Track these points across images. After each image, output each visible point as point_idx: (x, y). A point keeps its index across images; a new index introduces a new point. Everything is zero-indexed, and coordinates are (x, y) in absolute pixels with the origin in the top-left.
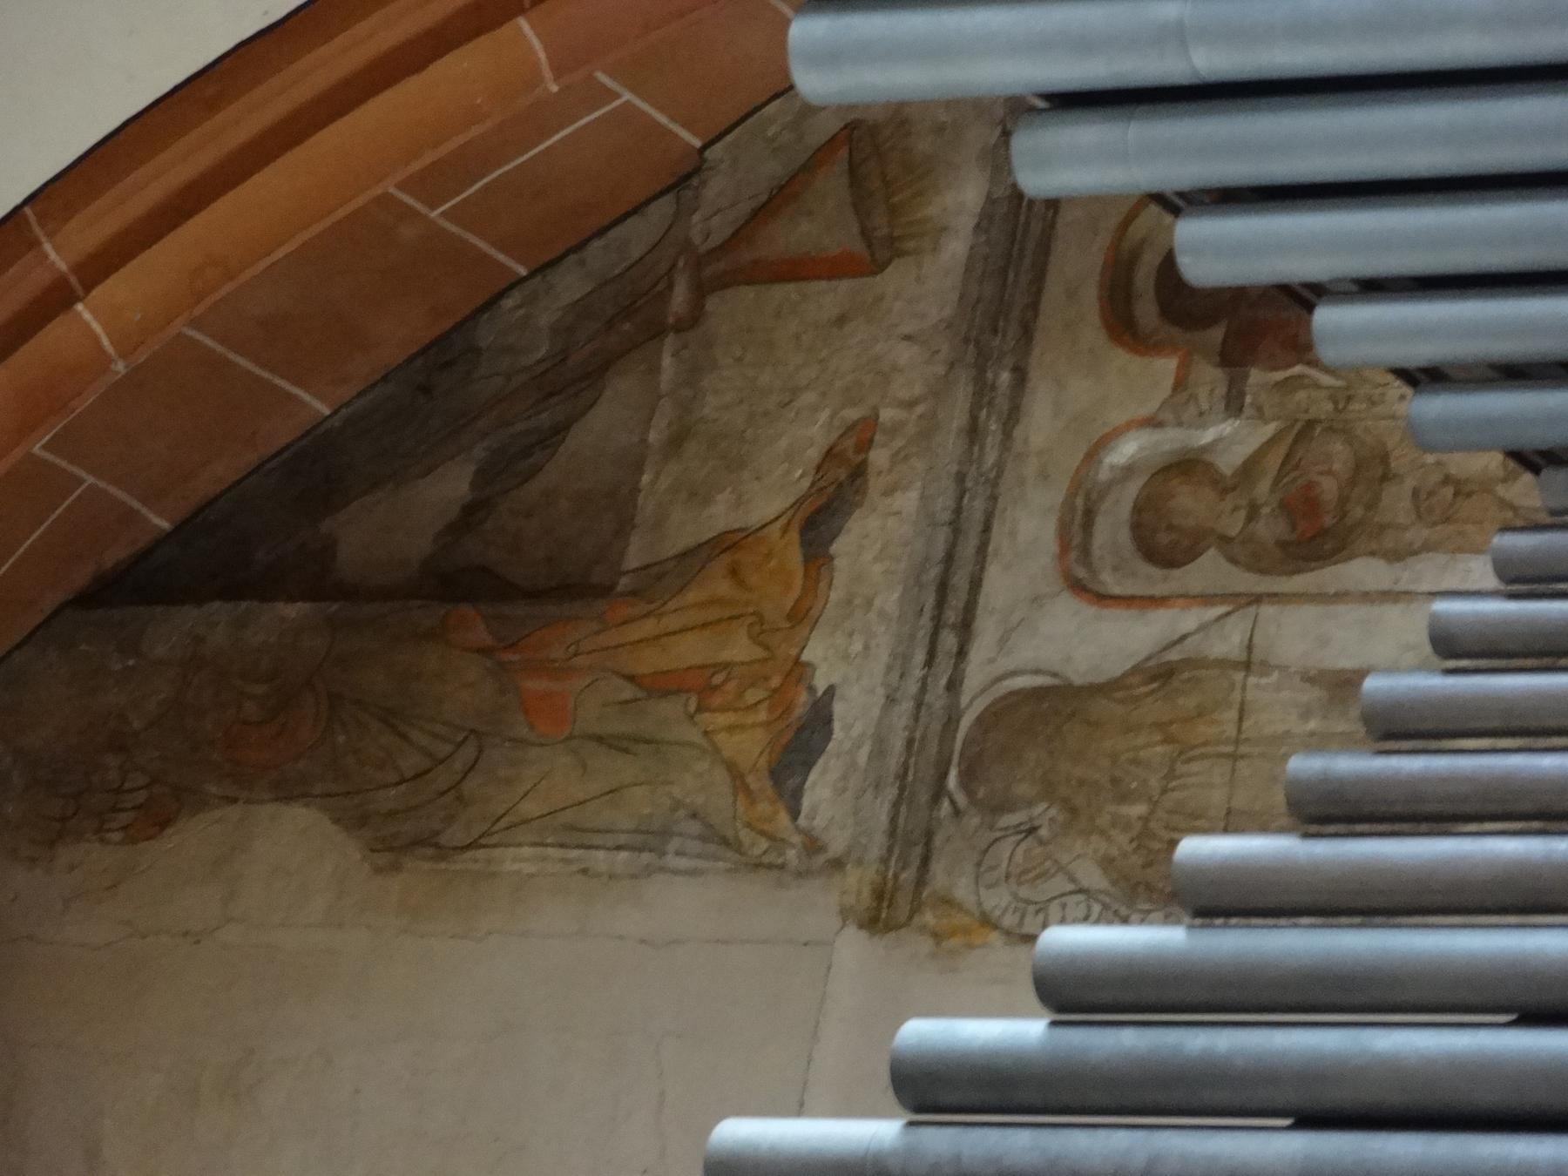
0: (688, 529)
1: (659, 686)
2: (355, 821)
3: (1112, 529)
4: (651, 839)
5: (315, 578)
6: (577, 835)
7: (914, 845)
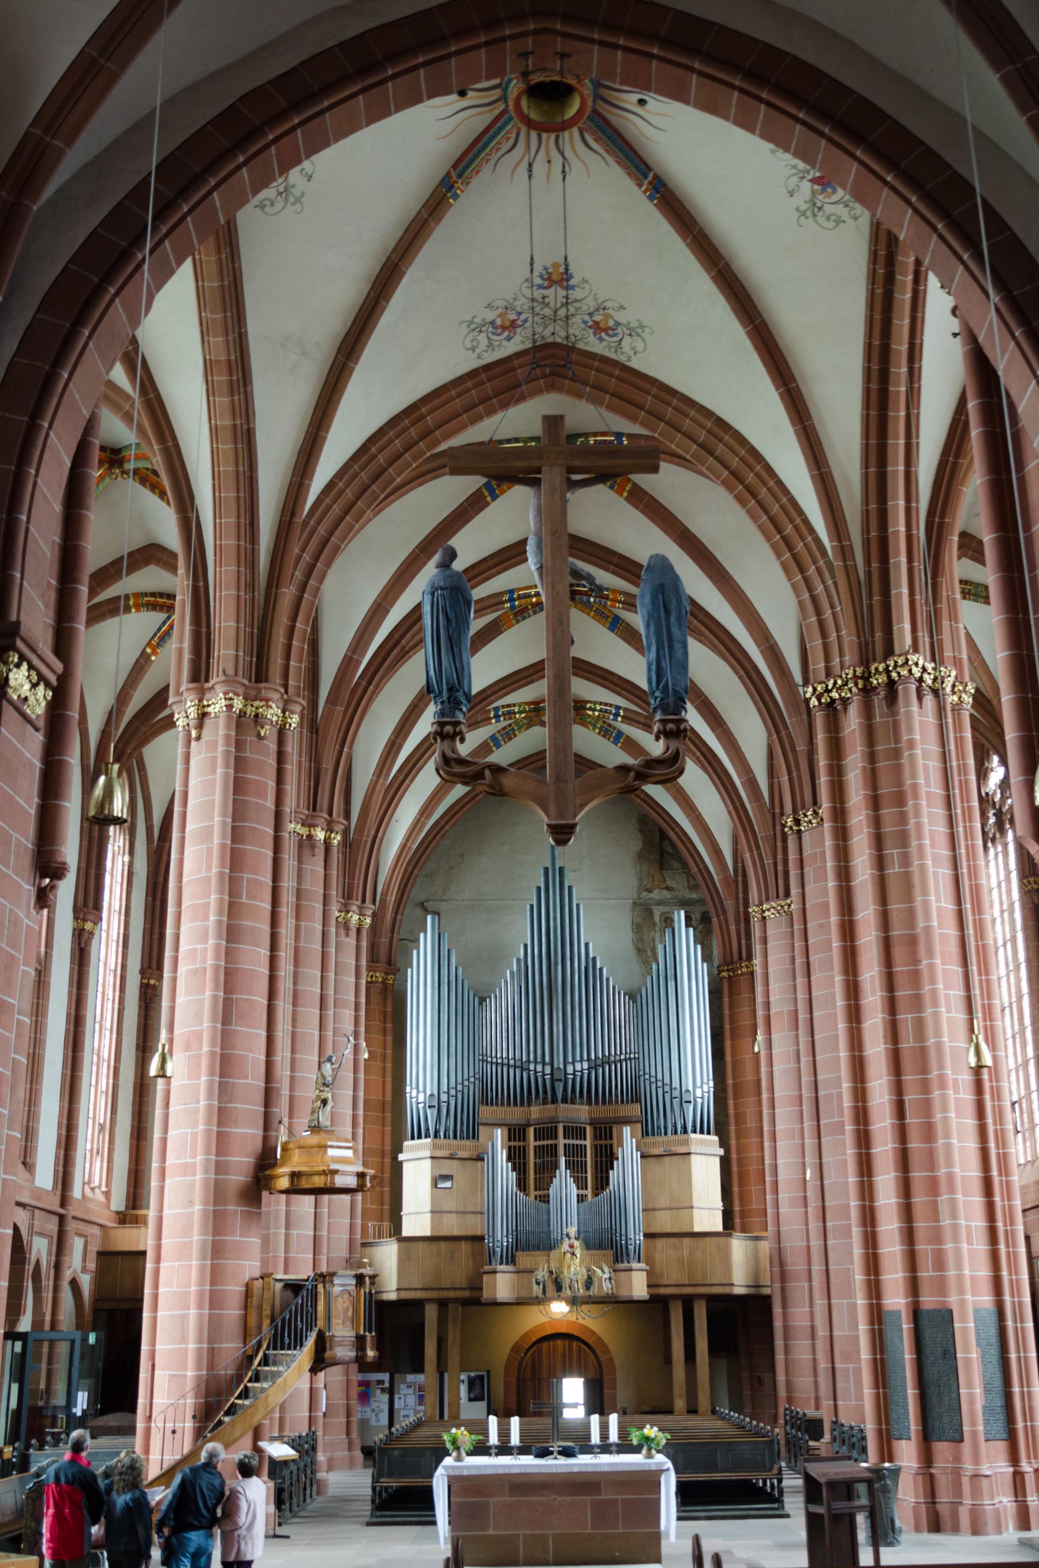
0: (666, 876)
4: (641, 879)
5: (661, 841)
6: (641, 871)
7: (640, 905)
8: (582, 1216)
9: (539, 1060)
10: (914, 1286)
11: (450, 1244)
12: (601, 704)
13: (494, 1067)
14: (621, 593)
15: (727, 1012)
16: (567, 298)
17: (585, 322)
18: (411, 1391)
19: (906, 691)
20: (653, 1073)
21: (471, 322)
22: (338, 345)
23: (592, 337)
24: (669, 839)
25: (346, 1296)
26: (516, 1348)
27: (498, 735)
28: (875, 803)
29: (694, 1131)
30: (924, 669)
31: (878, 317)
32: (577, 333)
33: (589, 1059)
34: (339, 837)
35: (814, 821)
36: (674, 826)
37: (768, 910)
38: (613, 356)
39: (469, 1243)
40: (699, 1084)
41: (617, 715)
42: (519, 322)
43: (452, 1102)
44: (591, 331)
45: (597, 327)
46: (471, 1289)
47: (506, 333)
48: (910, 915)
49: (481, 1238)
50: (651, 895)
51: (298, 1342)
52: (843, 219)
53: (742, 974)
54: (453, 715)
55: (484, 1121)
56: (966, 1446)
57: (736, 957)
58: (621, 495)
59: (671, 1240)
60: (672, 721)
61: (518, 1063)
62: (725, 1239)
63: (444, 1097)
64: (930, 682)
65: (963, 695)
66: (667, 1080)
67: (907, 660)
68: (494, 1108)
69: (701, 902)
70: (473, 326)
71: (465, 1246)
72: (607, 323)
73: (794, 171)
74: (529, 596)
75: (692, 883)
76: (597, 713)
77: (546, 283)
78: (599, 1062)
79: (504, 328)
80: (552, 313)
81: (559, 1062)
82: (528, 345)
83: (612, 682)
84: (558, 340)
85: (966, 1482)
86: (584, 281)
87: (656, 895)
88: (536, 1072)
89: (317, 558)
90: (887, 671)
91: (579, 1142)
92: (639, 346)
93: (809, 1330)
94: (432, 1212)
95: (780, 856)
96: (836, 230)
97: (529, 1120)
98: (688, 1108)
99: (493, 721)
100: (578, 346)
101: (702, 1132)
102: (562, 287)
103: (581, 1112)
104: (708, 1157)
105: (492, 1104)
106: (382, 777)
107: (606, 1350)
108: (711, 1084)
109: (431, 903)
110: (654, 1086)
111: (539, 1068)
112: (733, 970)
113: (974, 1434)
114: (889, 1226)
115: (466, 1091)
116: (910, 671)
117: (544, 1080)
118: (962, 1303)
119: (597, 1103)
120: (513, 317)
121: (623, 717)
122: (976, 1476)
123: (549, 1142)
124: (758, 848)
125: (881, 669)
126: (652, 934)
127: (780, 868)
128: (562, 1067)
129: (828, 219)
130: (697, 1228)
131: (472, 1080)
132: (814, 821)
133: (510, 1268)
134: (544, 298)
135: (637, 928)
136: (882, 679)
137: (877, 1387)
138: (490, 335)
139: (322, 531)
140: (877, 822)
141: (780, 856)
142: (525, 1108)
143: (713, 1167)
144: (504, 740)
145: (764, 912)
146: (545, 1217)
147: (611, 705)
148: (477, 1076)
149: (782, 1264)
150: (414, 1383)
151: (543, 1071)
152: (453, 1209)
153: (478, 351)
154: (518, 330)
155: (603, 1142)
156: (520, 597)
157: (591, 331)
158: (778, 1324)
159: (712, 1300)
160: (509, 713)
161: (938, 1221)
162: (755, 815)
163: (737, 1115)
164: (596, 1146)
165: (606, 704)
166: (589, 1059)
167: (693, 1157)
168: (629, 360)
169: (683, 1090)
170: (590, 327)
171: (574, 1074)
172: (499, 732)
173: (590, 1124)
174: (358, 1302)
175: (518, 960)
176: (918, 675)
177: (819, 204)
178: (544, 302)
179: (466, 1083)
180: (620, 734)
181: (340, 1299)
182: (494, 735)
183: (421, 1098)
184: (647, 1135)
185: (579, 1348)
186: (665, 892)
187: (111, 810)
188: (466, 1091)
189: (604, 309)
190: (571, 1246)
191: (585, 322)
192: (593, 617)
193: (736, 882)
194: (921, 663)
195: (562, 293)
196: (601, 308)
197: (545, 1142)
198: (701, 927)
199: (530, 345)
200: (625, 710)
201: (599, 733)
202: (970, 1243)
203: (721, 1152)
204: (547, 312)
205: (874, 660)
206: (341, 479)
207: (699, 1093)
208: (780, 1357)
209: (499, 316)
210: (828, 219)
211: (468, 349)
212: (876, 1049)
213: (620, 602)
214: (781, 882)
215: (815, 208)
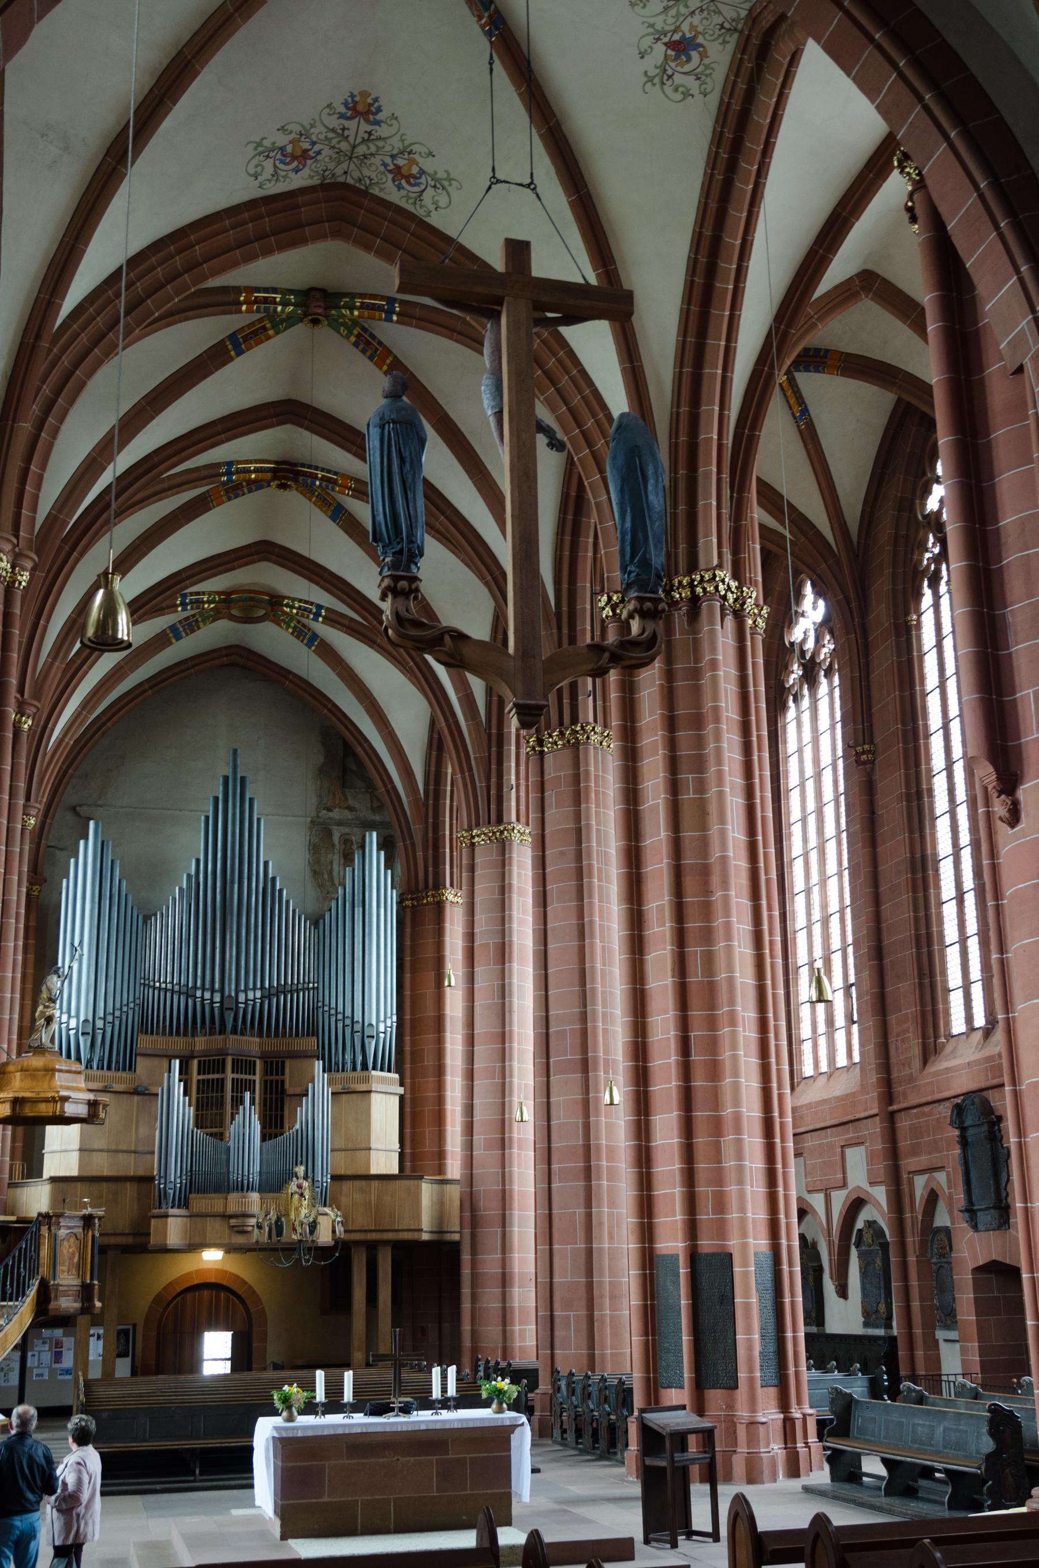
1: (334, 795)
3: (347, 837)
4: (320, 796)
7: (319, 824)
8: (264, 1156)
9: (207, 986)
10: (692, 1229)
11: (112, 1186)
12: (300, 601)
13: (156, 992)
14: (352, 479)
16: (370, 133)
17: (385, 165)
18: (47, 1347)
19: (711, 608)
20: (333, 1005)
21: (259, 144)
22: (108, 145)
23: (390, 183)
24: (354, 754)
25: (72, 1240)
26: (158, 1299)
27: (178, 625)
28: (671, 724)
29: (374, 1068)
30: (729, 588)
31: (713, 205)
32: (373, 175)
33: (262, 987)
34: (30, 722)
35: (560, 742)
36: (362, 741)
37: (478, 836)
38: (410, 208)
39: (135, 1185)
40: (382, 1018)
41: (317, 615)
42: (311, 153)
44: (390, 176)
45: (398, 173)
46: (135, 1235)
47: (295, 163)
48: (704, 844)
49: (150, 1179)
50: (331, 814)
51: (20, 1293)
52: (691, 92)
53: (428, 903)
54: (409, 570)
55: (143, 1051)
56: (741, 1394)
57: (421, 885)
58: (381, 369)
59: (357, 1183)
60: (649, 599)
61: (184, 989)
62: (416, 1182)
63: (100, 1024)
64: (731, 601)
65: (759, 620)
66: (348, 1013)
67: (715, 576)
68: (155, 1037)
70: (260, 149)
71: (130, 1189)
72: (410, 169)
73: (650, 30)
74: (248, 471)
75: (376, 804)
76: (295, 611)
77: (350, 113)
78: (273, 991)
79: (294, 157)
80: (349, 148)
81: (230, 989)
82: (316, 181)
83: (322, 577)
84: (350, 181)
85: (742, 1432)
86: (394, 117)
87: (336, 814)
88: (203, 999)
89: (58, 392)
90: (692, 585)
91: (248, 1077)
92: (443, 200)
93: (500, 1276)
94: (80, 1150)
95: (493, 780)
96: (682, 103)
97: (192, 1052)
98: (370, 1043)
99: (180, 609)
100: (371, 191)
101: (382, 1070)
102: (367, 121)
103: (252, 1044)
104: (388, 1096)
105: (152, 1033)
106: (59, 660)
107: (258, 1300)
108: (395, 1018)
109: (85, 808)
110: (333, 1019)
111: (207, 995)
112: (417, 899)
113: (751, 1380)
114: (668, 1167)
115: (124, 1017)
116: (716, 588)
117: (212, 1009)
118: (745, 1246)
119: (268, 1035)
120: (306, 146)
121: (324, 618)
122: (752, 1424)
123: (216, 1076)
124: (470, 769)
125: (685, 582)
126: (330, 856)
127: (493, 792)
128: (233, 994)
129: (676, 90)
130: (374, 1171)
131: (132, 1005)
132: (560, 742)
134: (344, 129)
135: (315, 849)
136: (686, 593)
137: (646, 1334)
138: (277, 162)
139: (66, 361)
140: (672, 744)
141: (493, 780)
142: (189, 1039)
143: (392, 1105)
144: (185, 630)
145: (473, 837)
146: (224, 1157)
147: (312, 604)
148: (137, 1002)
149: (473, 1208)
150: (51, 1339)
151: (212, 999)
152: (105, 1147)
153: (261, 178)
154: (309, 162)
155: (274, 1078)
156: (238, 471)
157: (390, 176)
158: (466, 1271)
160: (197, 601)
161: (720, 1162)
162: (470, 734)
163: (413, 1052)
164: (266, 1082)
165: (306, 602)
166: (262, 987)
167: (373, 1095)
168: (429, 214)
169: (366, 1024)
170: (390, 171)
171: (246, 1003)
172: (180, 622)
173: (260, 1058)
174: (85, 1247)
175: (189, 876)
176: (723, 593)
177: (670, 72)
178: (342, 134)
179: (125, 1009)
180: (315, 636)
181: (66, 1243)
182: (174, 625)
183: (73, 1023)
185: (228, 1300)
186: (346, 812)
187: (115, 630)
188: (124, 1017)
189: (410, 153)
190: (300, 1187)
191: (385, 165)
192: (314, 503)
193: (426, 806)
194: (727, 580)
195: (365, 127)
196: (406, 151)
197: (210, 1076)
199: (318, 182)
200: (328, 610)
201: (292, 634)
202: (752, 1187)
203: (401, 1090)
204: (344, 146)
205: (677, 573)
206: (92, 304)
207: (382, 1028)
208: (466, 1305)
209: (290, 142)
210: (676, 90)
211: (251, 175)
212: (661, 982)
213: (350, 488)
214: (493, 807)
215: (665, 75)
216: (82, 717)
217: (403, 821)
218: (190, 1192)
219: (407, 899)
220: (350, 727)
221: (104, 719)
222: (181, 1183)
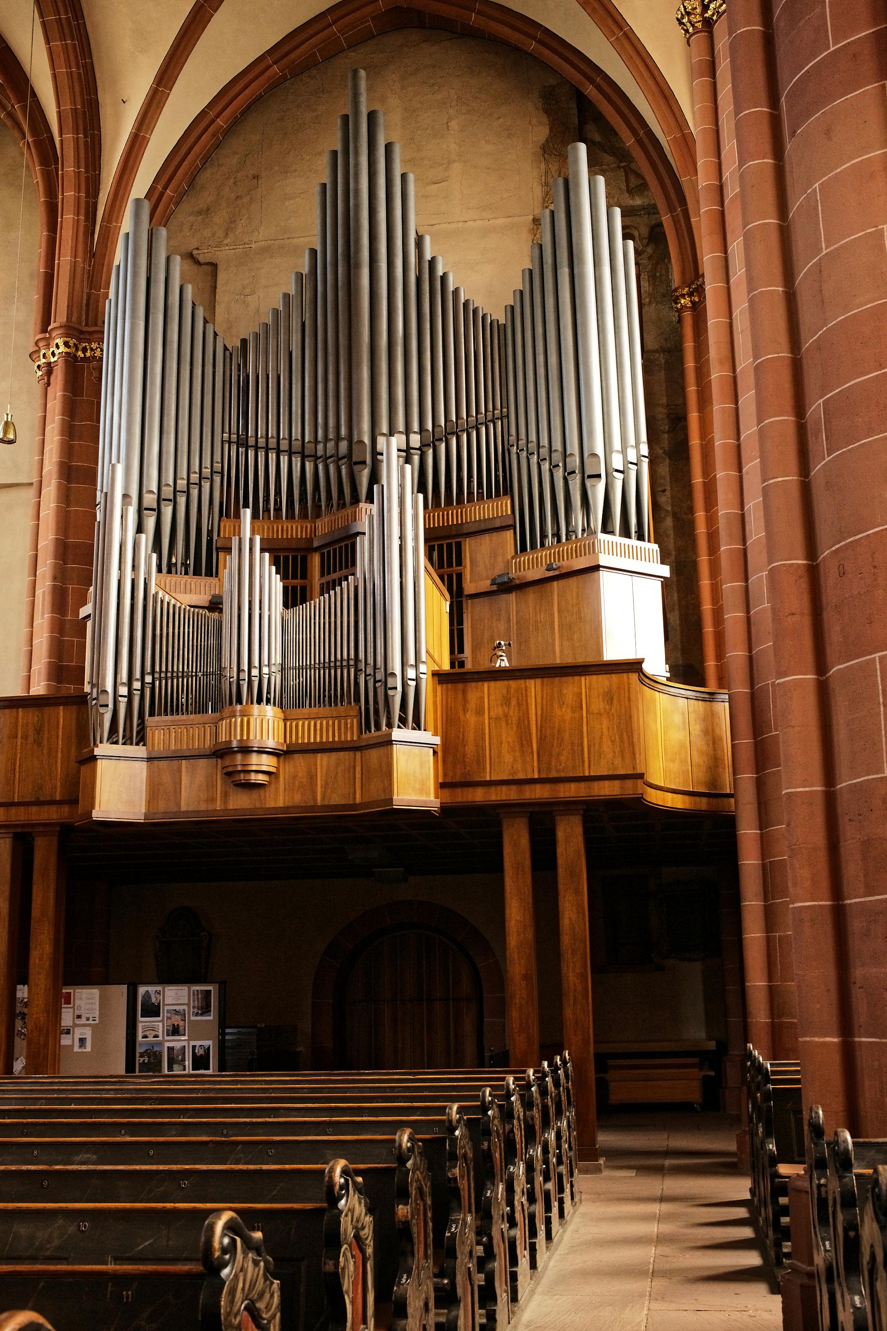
2: (547, 141)
8: (292, 636)
9: (331, 436)
15: (690, 364)
29: (606, 528)
33: (422, 430)
36: (592, 74)
40: (617, 444)
43: (167, 511)
61: (296, 445)
69: (652, 210)
75: (634, 182)
108: (644, 450)
115: (195, 492)
128: (366, 439)
133: (140, 751)
146: (212, 641)
158: (750, 861)
159: (594, 813)
167: (603, 575)
169: (586, 455)
184: (523, 549)
198: (649, 250)
207: (617, 462)
208: (754, 934)
216: (158, 97)
217: (668, 181)
218: (152, 714)
219: (683, 296)
220: (576, 61)
221: (212, 114)
222: (130, 696)
